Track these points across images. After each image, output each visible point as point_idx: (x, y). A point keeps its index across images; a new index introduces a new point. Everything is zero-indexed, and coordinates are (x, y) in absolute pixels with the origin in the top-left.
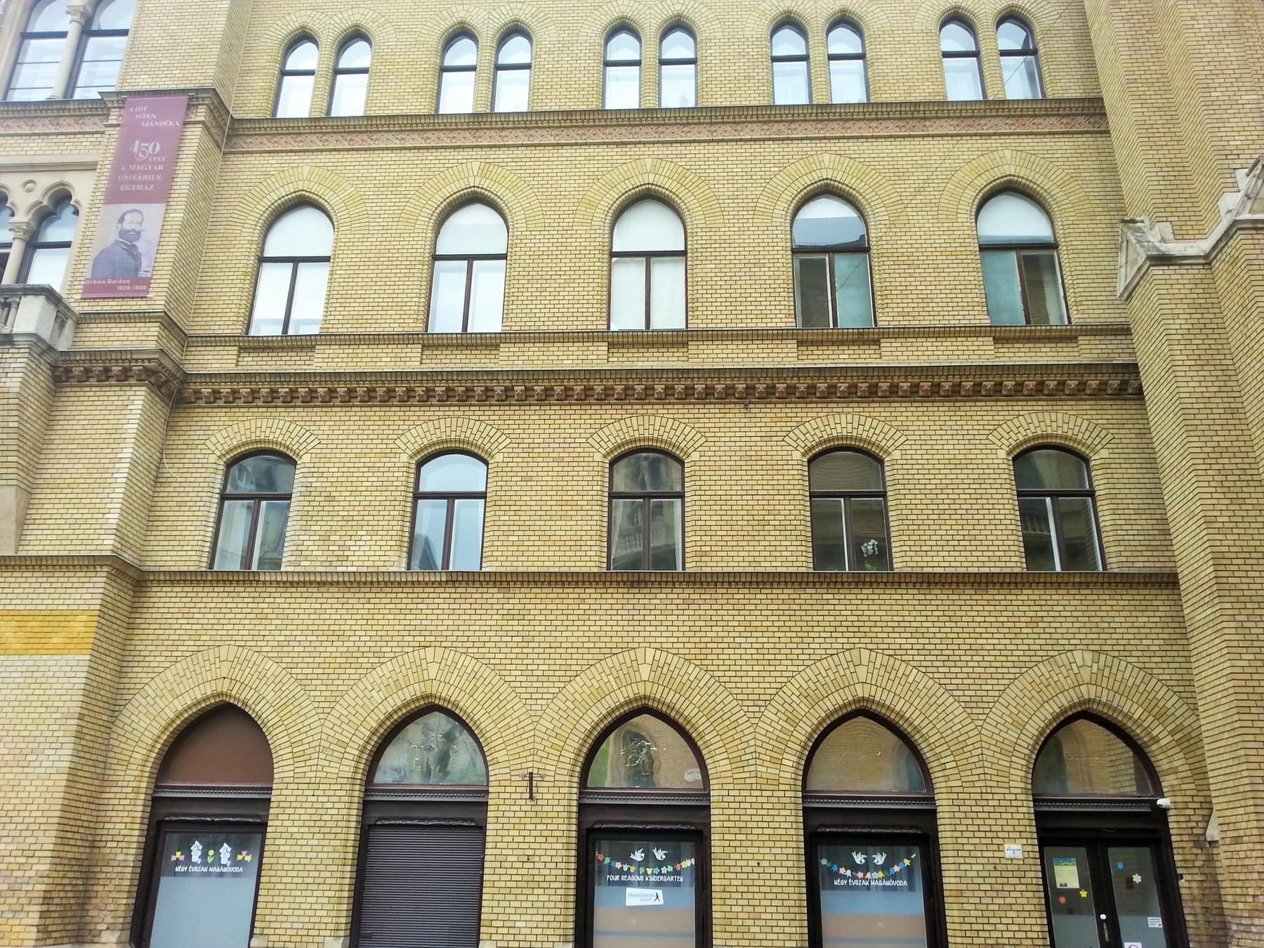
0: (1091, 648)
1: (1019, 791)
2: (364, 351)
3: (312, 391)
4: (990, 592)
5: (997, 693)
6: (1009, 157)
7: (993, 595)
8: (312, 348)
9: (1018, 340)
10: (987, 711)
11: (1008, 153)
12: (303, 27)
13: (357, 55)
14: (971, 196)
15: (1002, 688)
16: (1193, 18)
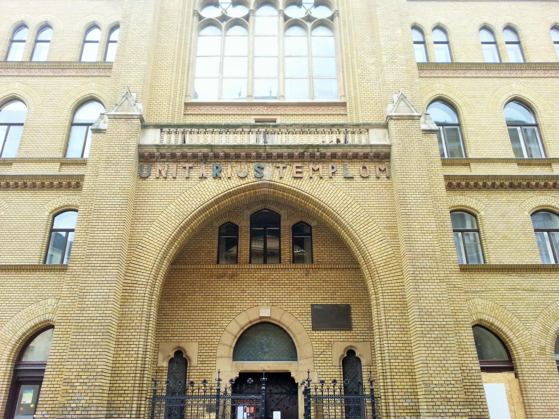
0: (56, 297)
1: (4, 360)
2: (41, 165)
3: (34, 183)
4: (22, 273)
5: (10, 317)
6: (90, 86)
7: (24, 275)
8: (11, 164)
9: (72, 164)
10: (3, 325)
11: (94, 84)
12: (46, 22)
13: (46, 35)
14: (72, 102)
15: (13, 315)
16: (134, 30)
